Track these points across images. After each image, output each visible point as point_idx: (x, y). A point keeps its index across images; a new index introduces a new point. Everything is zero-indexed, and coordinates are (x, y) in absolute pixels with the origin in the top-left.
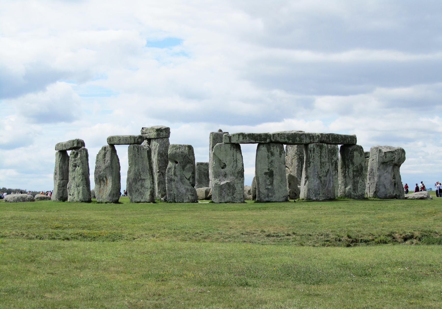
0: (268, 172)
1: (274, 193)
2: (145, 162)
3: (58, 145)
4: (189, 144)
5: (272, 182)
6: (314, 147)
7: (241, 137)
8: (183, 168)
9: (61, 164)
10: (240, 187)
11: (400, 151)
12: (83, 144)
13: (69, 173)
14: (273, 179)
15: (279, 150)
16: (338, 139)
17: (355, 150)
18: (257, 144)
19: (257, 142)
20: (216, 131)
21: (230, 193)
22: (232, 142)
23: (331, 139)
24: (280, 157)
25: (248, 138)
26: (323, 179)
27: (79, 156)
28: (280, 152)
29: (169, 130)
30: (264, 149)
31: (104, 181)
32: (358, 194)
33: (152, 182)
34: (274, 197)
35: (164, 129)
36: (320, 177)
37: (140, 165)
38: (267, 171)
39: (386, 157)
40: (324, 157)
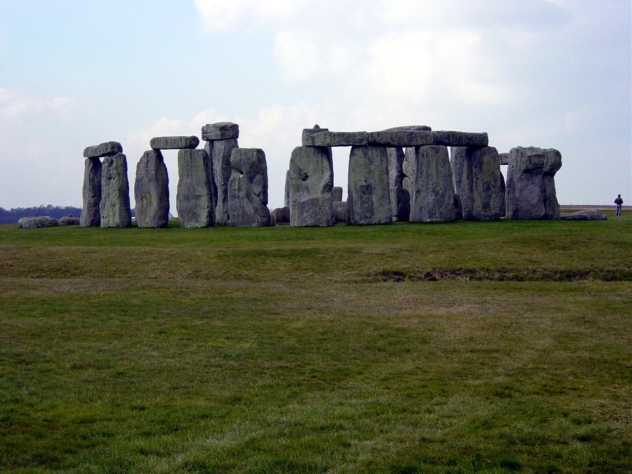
1: (373, 214)
3: (87, 150)
8: (251, 179)
9: (92, 176)
11: (552, 153)
12: (120, 148)
13: (102, 188)
14: (371, 193)
18: (351, 147)
19: (350, 144)
20: (311, 127)
22: (316, 145)
23: (451, 139)
27: (114, 165)
29: (238, 128)
30: (359, 152)
31: (147, 199)
32: (490, 214)
33: (209, 200)
34: (372, 219)
38: (364, 184)
39: (530, 162)
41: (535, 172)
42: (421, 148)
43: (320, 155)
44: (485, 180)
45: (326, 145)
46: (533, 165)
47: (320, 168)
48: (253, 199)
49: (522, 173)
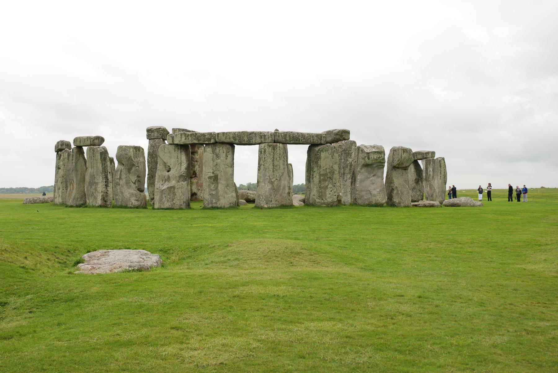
0: (212, 177)
1: (219, 200)
2: (98, 164)
4: (136, 145)
6: (266, 148)
7: (183, 139)
8: (129, 170)
11: (400, 151)
14: (217, 183)
15: (225, 150)
17: (322, 151)
22: (175, 143)
23: (288, 139)
24: (226, 159)
25: (190, 138)
32: (326, 201)
37: (95, 168)
38: (212, 175)
39: (369, 158)
46: (372, 160)
47: (180, 162)
48: (130, 186)
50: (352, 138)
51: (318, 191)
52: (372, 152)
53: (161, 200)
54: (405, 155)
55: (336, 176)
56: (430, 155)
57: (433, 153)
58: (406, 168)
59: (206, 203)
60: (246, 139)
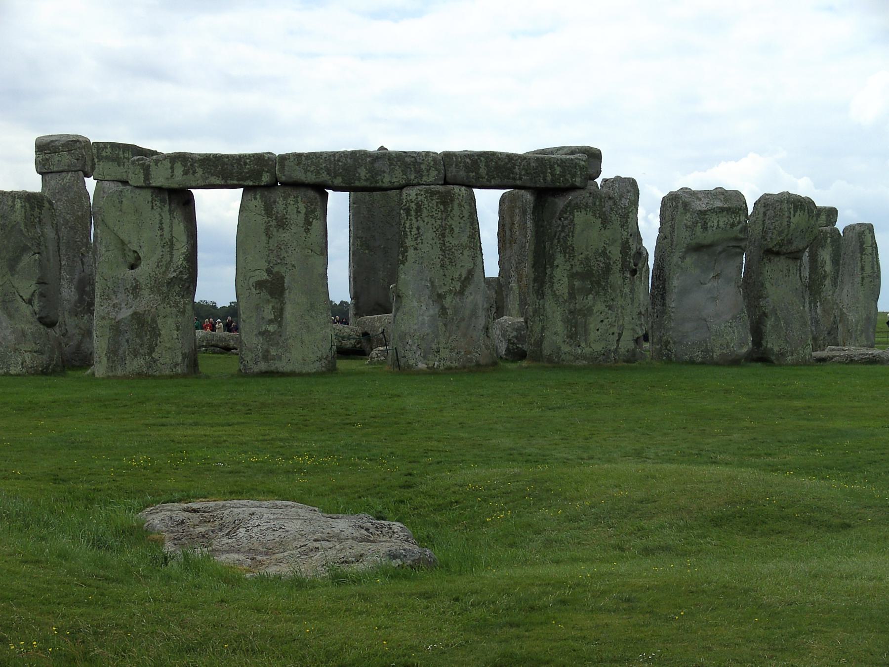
0: (266, 281)
5: (282, 311)
7: (179, 170)
10: (174, 326)
11: (785, 206)
14: (283, 303)
16: (511, 170)
17: (578, 207)
19: (230, 182)
21: (141, 345)
22: (154, 184)
23: (483, 171)
24: (307, 231)
25: (200, 172)
26: (448, 302)
28: (306, 214)
30: (257, 203)
32: (587, 350)
35: (63, 145)
36: (441, 297)
38: (265, 276)
39: (705, 228)
40: (456, 230)
41: (724, 251)
42: (405, 191)
43: (167, 207)
44: (574, 271)
45: (175, 186)
47: (167, 236)
48: (17, 309)
49: (686, 252)
50: (608, 171)
51: (566, 321)
52: (713, 211)
53: (113, 353)
54: (798, 219)
55: (616, 278)
56: (823, 217)
57: (832, 213)
58: (795, 256)
59: (249, 357)
60: (363, 172)
